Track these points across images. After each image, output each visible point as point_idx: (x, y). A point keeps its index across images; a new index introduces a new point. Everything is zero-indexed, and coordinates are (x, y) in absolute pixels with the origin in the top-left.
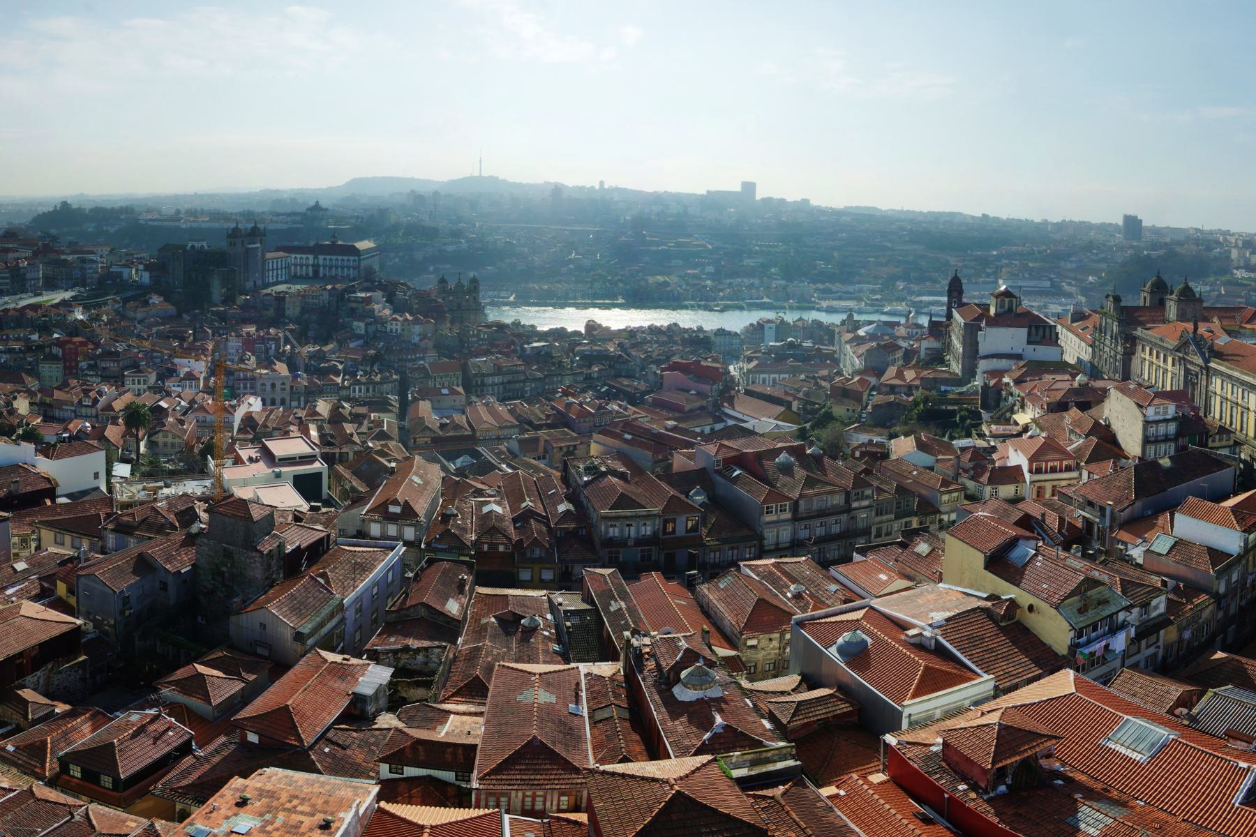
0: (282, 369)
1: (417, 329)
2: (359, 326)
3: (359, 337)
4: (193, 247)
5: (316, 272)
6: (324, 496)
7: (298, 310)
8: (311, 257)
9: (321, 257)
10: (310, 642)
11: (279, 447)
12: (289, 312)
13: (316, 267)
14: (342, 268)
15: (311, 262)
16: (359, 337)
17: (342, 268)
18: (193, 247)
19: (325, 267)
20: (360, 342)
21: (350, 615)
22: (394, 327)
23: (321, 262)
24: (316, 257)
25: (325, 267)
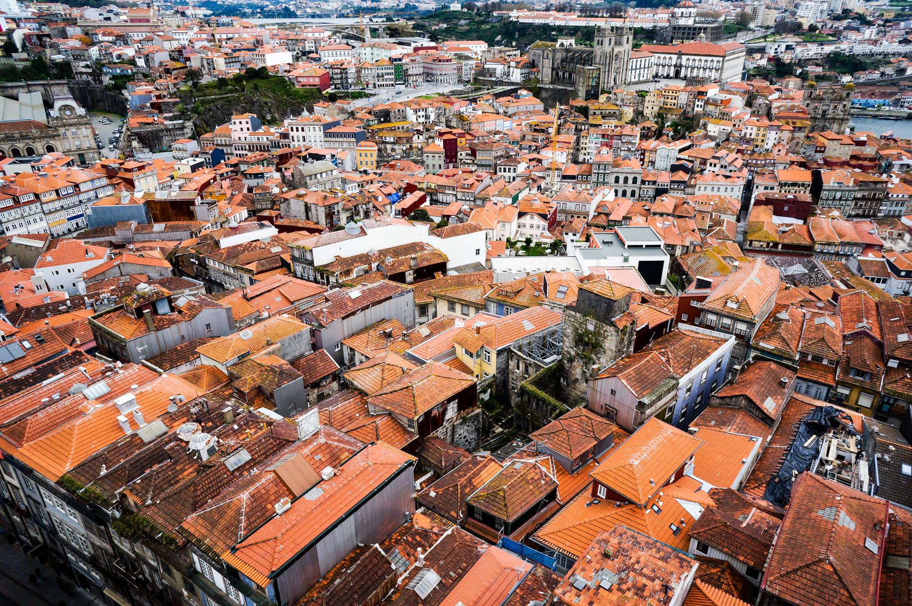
0: (634, 165)
1: (772, 136)
2: (713, 129)
3: (713, 139)
4: (562, 45)
5: (677, 74)
6: (663, 282)
7: (656, 109)
8: (674, 57)
9: (684, 58)
10: (648, 412)
11: (629, 235)
12: (647, 112)
13: (678, 68)
14: (705, 69)
15: (674, 62)
16: (713, 139)
17: (705, 69)
18: (562, 45)
19: (687, 68)
20: (713, 144)
21: (683, 395)
22: (749, 131)
23: (684, 63)
24: (679, 57)
25: (687, 68)
